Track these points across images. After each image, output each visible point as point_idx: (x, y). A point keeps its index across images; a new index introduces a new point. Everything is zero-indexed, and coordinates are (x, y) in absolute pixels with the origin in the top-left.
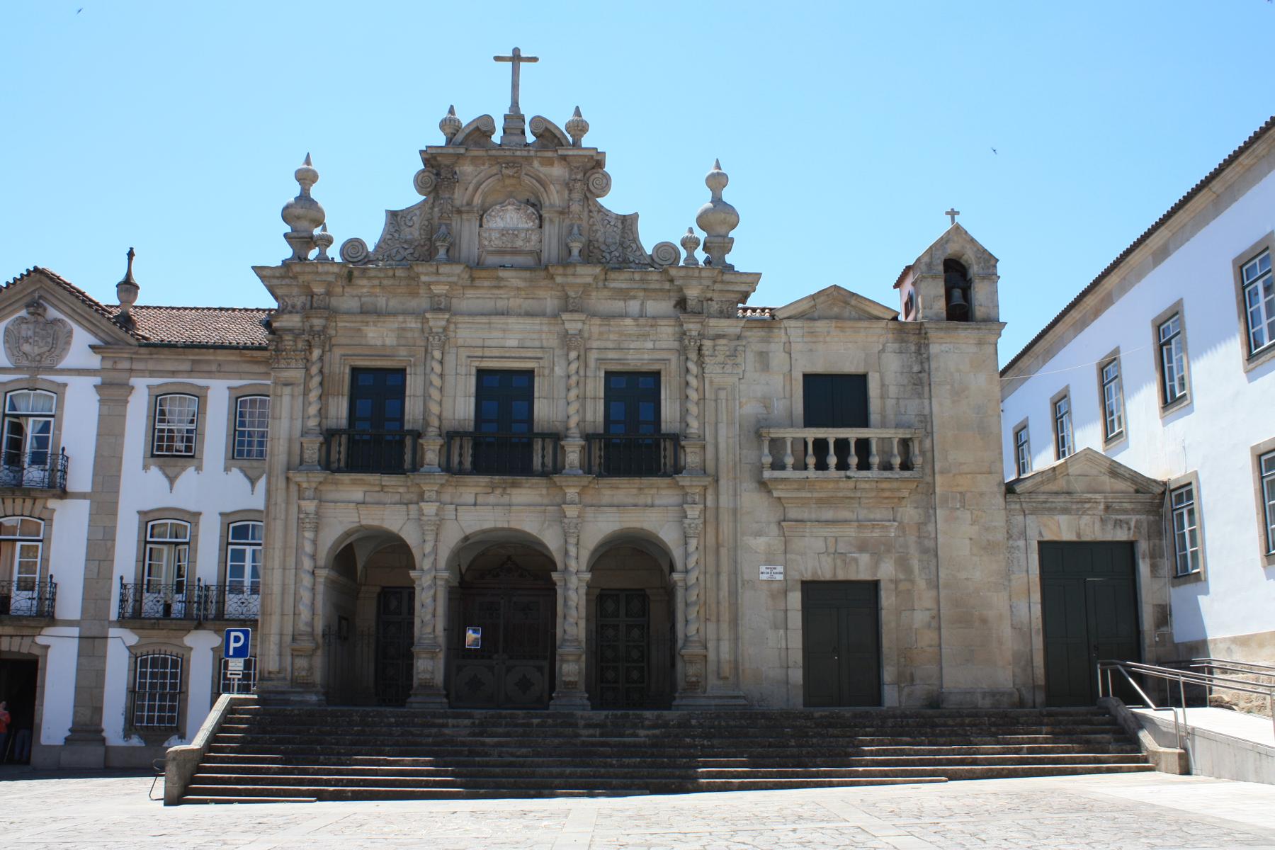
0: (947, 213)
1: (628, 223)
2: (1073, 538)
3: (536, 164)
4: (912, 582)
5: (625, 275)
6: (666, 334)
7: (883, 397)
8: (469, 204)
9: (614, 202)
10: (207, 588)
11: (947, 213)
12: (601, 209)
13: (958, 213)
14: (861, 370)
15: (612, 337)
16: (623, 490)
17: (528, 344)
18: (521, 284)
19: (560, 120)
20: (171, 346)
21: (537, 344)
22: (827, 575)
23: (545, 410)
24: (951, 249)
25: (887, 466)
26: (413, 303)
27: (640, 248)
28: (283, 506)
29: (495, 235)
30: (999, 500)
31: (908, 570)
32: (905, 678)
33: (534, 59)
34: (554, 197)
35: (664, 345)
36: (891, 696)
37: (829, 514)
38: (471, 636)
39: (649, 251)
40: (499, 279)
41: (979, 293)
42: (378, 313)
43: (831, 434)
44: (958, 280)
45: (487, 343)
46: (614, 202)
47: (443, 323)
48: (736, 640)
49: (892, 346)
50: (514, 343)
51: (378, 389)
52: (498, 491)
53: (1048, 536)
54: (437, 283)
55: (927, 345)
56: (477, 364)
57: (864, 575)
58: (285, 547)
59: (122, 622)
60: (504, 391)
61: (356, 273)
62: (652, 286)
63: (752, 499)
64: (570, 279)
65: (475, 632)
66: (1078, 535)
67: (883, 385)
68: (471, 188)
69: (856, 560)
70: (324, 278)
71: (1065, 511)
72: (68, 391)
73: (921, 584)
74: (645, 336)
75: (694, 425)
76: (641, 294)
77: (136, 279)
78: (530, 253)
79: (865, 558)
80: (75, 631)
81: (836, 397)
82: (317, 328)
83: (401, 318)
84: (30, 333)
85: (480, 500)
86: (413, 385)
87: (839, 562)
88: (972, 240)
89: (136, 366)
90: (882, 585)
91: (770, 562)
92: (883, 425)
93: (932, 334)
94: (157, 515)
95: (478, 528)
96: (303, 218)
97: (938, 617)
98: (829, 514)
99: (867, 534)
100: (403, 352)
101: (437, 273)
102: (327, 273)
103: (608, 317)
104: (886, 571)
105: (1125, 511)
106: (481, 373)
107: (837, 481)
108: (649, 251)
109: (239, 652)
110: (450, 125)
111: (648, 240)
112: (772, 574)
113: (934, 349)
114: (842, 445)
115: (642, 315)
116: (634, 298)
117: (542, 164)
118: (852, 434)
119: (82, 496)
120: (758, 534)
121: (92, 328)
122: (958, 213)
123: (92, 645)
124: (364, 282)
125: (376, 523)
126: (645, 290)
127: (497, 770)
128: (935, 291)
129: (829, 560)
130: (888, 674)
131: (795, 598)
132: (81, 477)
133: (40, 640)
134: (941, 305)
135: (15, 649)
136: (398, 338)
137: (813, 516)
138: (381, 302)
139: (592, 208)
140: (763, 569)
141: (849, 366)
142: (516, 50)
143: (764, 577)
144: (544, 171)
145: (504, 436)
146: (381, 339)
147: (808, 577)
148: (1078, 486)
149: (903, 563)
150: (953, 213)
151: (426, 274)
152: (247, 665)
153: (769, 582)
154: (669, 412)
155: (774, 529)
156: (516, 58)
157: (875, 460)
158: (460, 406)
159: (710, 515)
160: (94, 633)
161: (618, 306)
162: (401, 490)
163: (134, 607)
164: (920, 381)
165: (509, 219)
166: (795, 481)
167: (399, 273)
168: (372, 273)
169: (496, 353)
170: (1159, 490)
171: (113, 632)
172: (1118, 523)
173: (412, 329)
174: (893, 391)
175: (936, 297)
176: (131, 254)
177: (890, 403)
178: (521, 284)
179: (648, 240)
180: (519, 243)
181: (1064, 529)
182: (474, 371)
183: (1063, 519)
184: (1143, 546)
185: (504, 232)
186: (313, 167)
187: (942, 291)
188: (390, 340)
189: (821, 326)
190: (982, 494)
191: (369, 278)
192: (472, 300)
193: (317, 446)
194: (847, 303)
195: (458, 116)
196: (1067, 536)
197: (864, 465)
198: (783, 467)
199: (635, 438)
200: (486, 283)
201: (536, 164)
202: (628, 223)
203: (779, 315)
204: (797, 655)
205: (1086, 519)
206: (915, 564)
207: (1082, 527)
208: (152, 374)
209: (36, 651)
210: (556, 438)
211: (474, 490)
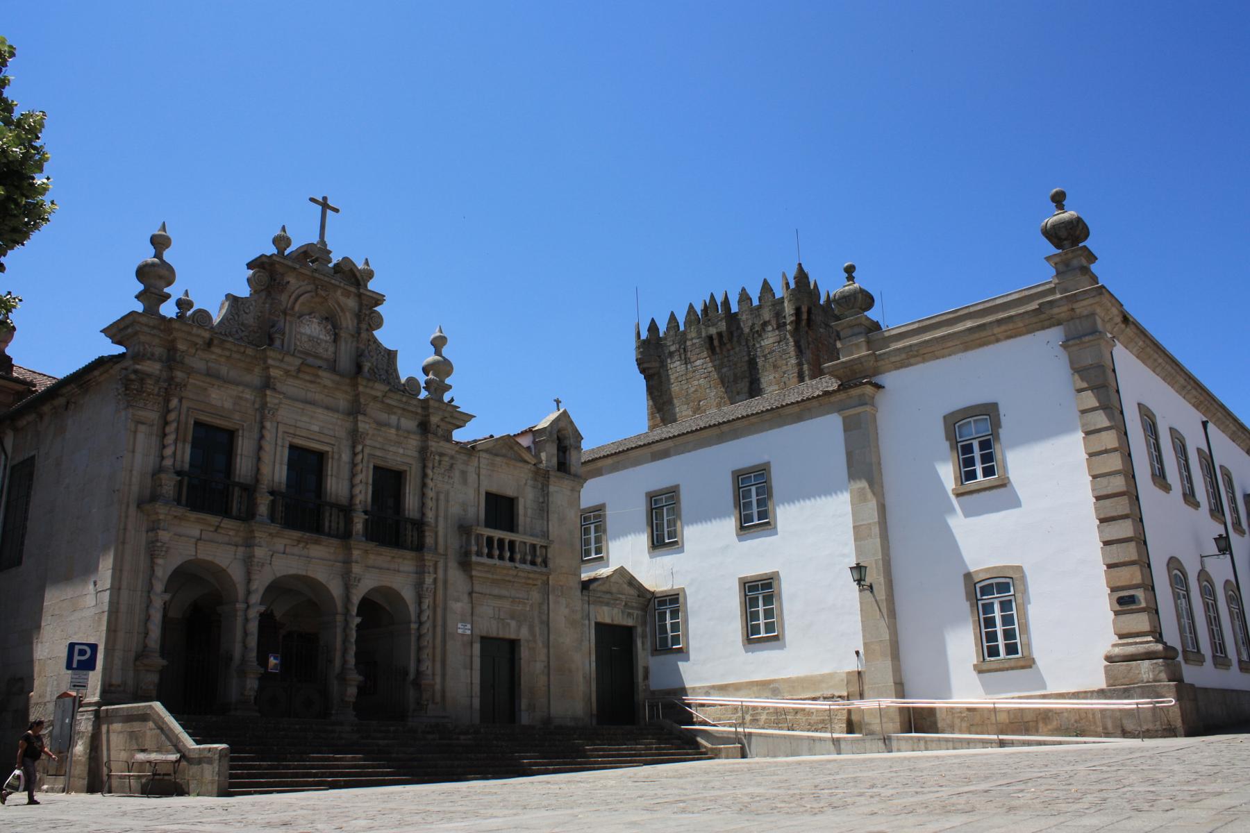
3: (339, 292)
5: (398, 397)
6: (414, 442)
7: (525, 515)
8: (293, 308)
15: (380, 439)
16: (383, 557)
17: (326, 431)
18: (329, 383)
21: (331, 433)
22: (494, 634)
23: (336, 486)
24: (562, 424)
25: (523, 561)
26: (248, 378)
27: (398, 377)
29: (304, 339)
31: (534, 636)
34: (348, 322)
35: (409, 453)
36: (525, 719)
37: (496, 591)
38: (272, 661)
39: (403, 380)
40: (317, 376)
42: (227, 381)
45: (299, 424)
47: (277, 401)
48: (444, 675)
49: (530, 482)
50: (316, 428)
51: (215, 442)
52: (301, 545)
54: (278, 368)
55: (548, 486)
57: (513, 636)
60: (308, 464)
61: (216, 342)
62: (411, 408)
63: (455, 576)
64: (368, 391)
65: (275, 658)
69: (509, 624)
70: (194, 339)
71: (607, 604)
73: (540, 644)
74: (399, 444)
75: (430, 516)
76: (400, 412)
78: (326, 360)
79: (513, 624)
81: (501, 509)
82: (178, 380)
83: (241, 388)
85: (288, 550)
86: (244, 446)
88: (572, 422)
90: (522, 642)
92: (525, 534)
93: (552, 479)
95: (285, 573)
96: (154, 278)
97: (548, 666)
98: (496, 591)
100: (237, 416)
101: (282, 361)
102: (198, 336)
103: (380, 424)
104: (524, 634)
105: (632, 608)
106: (293, 447)
107: (510, 569)
108: (403, 380)
112: (464, 629)
113: (552, 489)
115: (398, 428)
118: (507, 536)
120: (457, 600)
124: (218, 351)
125: (210, 558)
130: (524, 703)
131: (477, 647)
136: (235, 404)
138: (224, 370)
141: (510, 492)
142: (325, 198)
143: (460, 631)
144: (342, 299)
145: (304, 502)
146: (223, 401)
147: (484, 634)
148: (614, 590)
149: (531, 628)
151: (274, 359)
153: (463, 635)
154: (411, 502)
155: (466, 598)
156: (324, 205)
157: (518, 556)
158: (276, 471)
159: (440, 584)
161: (383, 417)
162: (231, 533)
164: (543, 508)
165: (312, 329)
166: (489, 566)
167: (250, 351)
168: (228, 346)
169: (304, 433)
170: (649, 596)
172: (629, 615)
173: (246, 400)
177: (528, 520)
178: (329, 383)
180: (321, 350)
182: (287, 445)
184: (639, 630)
185: (311, 338)
186: (169, 233)
188: (228, 405)
189: (498, 459)
191: (224, 349)
192: (292, 387)
193: (172, 483)
194: (511, 448)
196: (608, 620)
199: (392, 520)
200: (307, 377)
201: (339, 292)
203: (479, 448)
204: (477, 689)
205: (616, 610)
206: (537, 629)
210: (346, 510)
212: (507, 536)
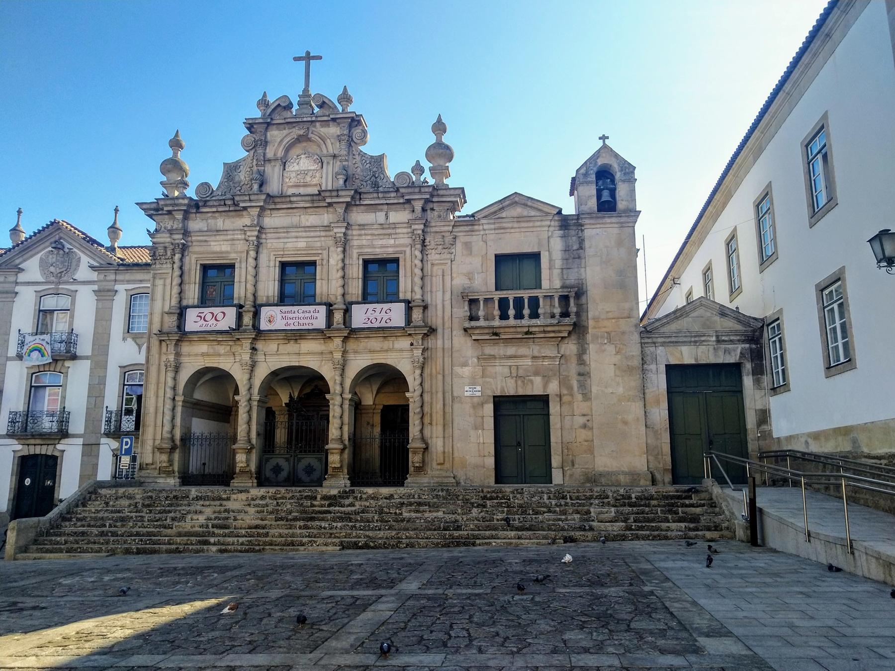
0: (600, 138)
1: (378, 161)
2: (693, 362)
4: (572, 395)
9: (370, 149)
10: (111, 412)
11: (600, 138)
12: (362, 155)
13: (608, 138)
14: (536, 250)
19: (333, 96)
20: (137, 265)
22: (512, 392)
28: (157, 356)
29: (293, 175)
30: (636, 337)
32: (569, 462)
33: (320, 58)
35: (402, 241)
41: (621, 191)
43: (511, 295)
44: (607, 184)
46: (370, 149)
53: (673, 361)
56: (280, 259)
58: (158, 383)
59: (108, 435)
66: (696, 359)
67: (551, 260)
68: (276, 144)
69: (531, 382)
72: (78, 295)
77: (118, 225)
78: (316, 185)
79: (538, 380)
80: (80, 441)
84: (54, 260)
87: (519, 382)
89: (119, 277)
91: (473, 383)
94: (131, 368)
99: (539, 362)
104: (553, 388)
109: (128, 452)
110: (263, 103)
111: (392, 171)
114: (519, 302)
116: (381, 210)
117: (322, 126)
119: (87, 358)
120: (465, 365)
121: (93, 255)
122: (608, 138)
123: (90, 450)
126: (387, 204)
127: (243, 532)
128: (590, 191)
129: (513, 381)
130: (555, 461)
131: (489, 408)
132: (85, 347)
133: (59, 447)
134: (593, 204)
135: (43, 452)
137: (502, 352)
139: (355, 152)
140: (467, 388)
142: (308, 53)
143: (467, 394)
149: (564, 382)
150: (604, 138)
152: (134, 459)
160: (92, 441)
163: (115, 427)
171: (104, 440)
174: (558, 263)
175: (590, 197)
176: (116, 210)
179: (392, 171)
180: (308, 179)
181: (687, 355)
183: (685, 349)
185: (299, 172)
187: (594, 192)
190: (623, 333)
195: (268, 98)
196: (688, 360)
197: (535, 315)
198: (477, 319)
202: (378, 161)
205: (702, 348)
207: (699, 354)
208: (129, 282)
209: (56, 454)
211: (277, 342)
212: (526, 294)
